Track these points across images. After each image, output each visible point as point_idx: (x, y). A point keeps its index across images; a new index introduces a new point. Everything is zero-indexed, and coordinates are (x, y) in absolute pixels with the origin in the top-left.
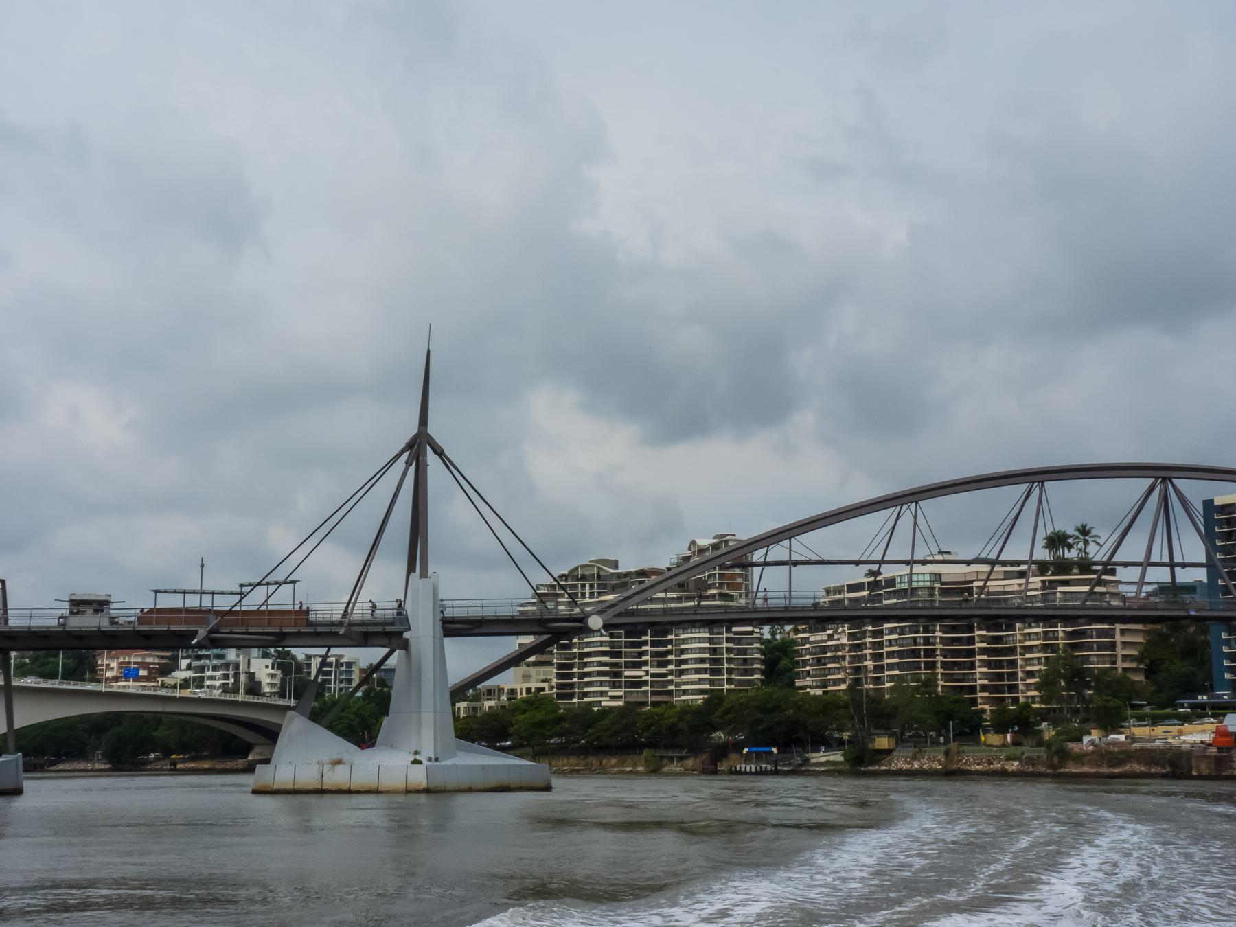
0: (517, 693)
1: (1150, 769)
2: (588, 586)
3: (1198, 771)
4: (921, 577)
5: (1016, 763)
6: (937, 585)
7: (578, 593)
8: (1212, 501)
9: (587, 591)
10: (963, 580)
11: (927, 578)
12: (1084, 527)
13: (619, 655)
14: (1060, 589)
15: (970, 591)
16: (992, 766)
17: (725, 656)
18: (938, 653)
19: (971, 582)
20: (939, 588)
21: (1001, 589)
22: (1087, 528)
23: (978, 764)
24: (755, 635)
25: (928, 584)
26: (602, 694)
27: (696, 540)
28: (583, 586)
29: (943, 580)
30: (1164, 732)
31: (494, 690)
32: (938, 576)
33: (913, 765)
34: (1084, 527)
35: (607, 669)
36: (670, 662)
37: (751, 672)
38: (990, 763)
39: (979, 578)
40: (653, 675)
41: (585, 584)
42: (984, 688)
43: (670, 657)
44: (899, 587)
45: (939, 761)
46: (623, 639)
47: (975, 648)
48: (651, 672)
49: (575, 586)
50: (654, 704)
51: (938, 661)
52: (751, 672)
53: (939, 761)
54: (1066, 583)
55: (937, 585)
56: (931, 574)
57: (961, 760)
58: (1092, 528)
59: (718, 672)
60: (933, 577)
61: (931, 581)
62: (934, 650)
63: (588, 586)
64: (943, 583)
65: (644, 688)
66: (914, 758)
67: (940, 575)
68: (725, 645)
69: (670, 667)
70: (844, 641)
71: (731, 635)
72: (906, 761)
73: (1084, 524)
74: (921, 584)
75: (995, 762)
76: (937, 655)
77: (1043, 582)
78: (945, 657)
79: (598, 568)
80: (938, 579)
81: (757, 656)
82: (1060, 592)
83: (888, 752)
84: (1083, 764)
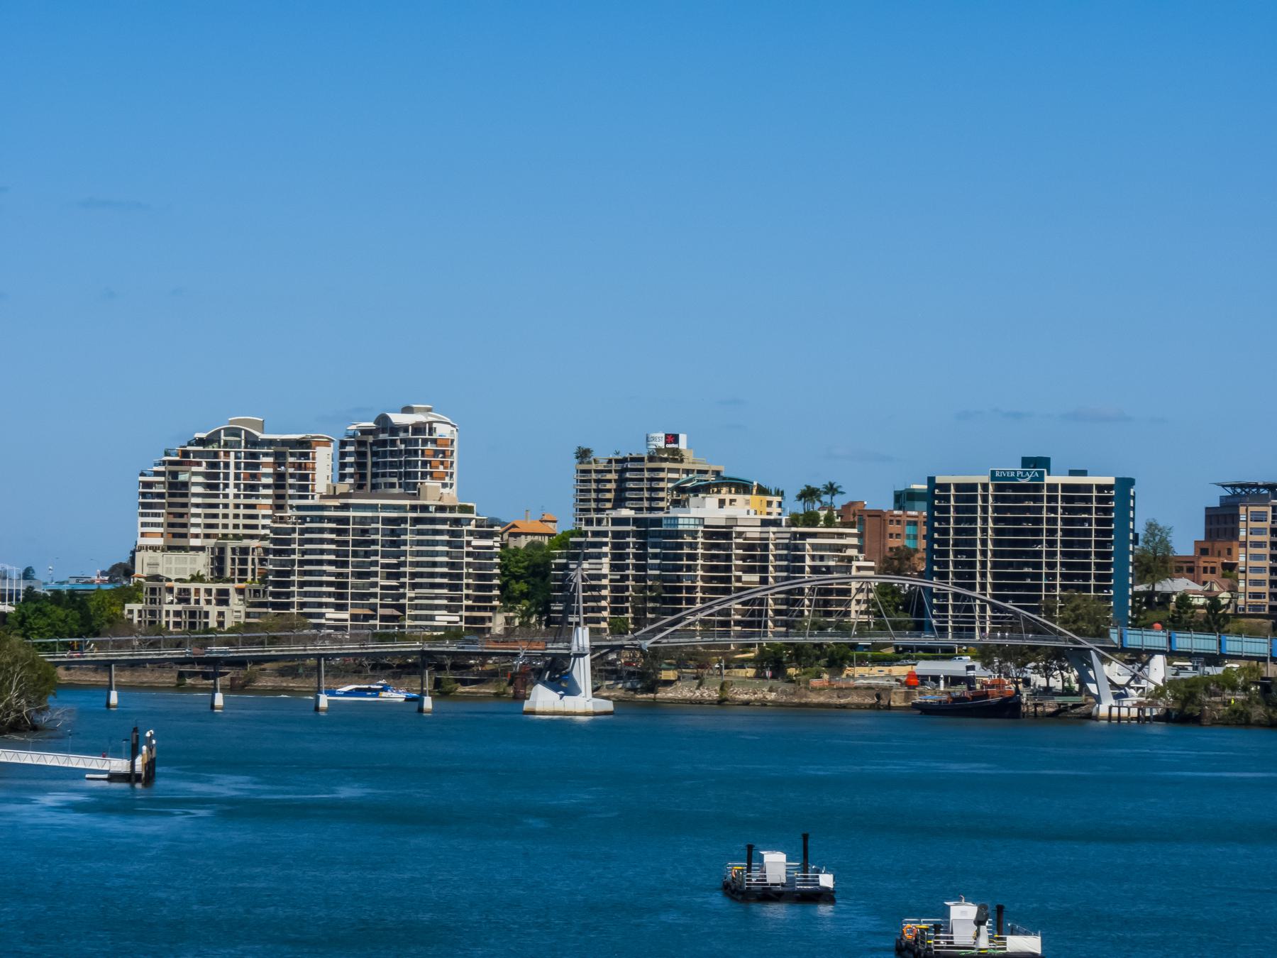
0: (190, 594)
1: (864, 700)
2: (232, 454)
3: (894, 702)
4: (686, 521)
5: (774, 694)
6: (701, 528)
7: (219, 462)
9: (232, 460)
10: (724, 524)
12: (832, 485)
13: (345, 564)
14: (809, 541)
15: (727, 536)
16: (756, 696)
17: (465, 571)
18: (699, 589)
19: (731, 527)
20: (702, 531)
21: (757, 535)
22: (835, 486)
23: (746, 694)
24: (496, 550)
25: (692, 528)
26: (327, 605)
27: (390, 415)
28: (227, 454)
29: (706, 524)
30: (879, 671)
31: (160, 589)
32: (702, 520)
33: (695, 693)
34: (832, 485)
35: (333, 579)
36: (404, 575)
37: (490, 588)
38: (755, 693)
39: (739, 524)
40: (383, 587)
41: (229, 452)
42: (738, 623)
43: (402, 569)
45: (715, 690)
46: (351, 548)
47: (731, 587)
48: (382, 583)
49: (216, 454)
50: (384, 618)
51: (697, 597)
52: (490, 588)
53: (715, 690)
54: (814, 535)
55: (701, 528)
56: (695, 518)
57: (733, 690)
58: (840, 486)
59: (457, 587)
62: (695, 587)
63: (232, 454)
64: (706, 527)
65: (372, 601)
66: (698, 688)
67: (703, 519)
68: (466, 560)
69: (402, 580)
70: (606, 570)
71: (471, 549)
72: (689, 689)
73: (832, 482)
74: (686, 528)
76: (697, 592)
77: (795, 533)
78: (704, 594)
79: (246, 431)
80: (702, 523)
81: (497, 571)
82: (809, 544)
83: (669, 683)
84: (821, 695)
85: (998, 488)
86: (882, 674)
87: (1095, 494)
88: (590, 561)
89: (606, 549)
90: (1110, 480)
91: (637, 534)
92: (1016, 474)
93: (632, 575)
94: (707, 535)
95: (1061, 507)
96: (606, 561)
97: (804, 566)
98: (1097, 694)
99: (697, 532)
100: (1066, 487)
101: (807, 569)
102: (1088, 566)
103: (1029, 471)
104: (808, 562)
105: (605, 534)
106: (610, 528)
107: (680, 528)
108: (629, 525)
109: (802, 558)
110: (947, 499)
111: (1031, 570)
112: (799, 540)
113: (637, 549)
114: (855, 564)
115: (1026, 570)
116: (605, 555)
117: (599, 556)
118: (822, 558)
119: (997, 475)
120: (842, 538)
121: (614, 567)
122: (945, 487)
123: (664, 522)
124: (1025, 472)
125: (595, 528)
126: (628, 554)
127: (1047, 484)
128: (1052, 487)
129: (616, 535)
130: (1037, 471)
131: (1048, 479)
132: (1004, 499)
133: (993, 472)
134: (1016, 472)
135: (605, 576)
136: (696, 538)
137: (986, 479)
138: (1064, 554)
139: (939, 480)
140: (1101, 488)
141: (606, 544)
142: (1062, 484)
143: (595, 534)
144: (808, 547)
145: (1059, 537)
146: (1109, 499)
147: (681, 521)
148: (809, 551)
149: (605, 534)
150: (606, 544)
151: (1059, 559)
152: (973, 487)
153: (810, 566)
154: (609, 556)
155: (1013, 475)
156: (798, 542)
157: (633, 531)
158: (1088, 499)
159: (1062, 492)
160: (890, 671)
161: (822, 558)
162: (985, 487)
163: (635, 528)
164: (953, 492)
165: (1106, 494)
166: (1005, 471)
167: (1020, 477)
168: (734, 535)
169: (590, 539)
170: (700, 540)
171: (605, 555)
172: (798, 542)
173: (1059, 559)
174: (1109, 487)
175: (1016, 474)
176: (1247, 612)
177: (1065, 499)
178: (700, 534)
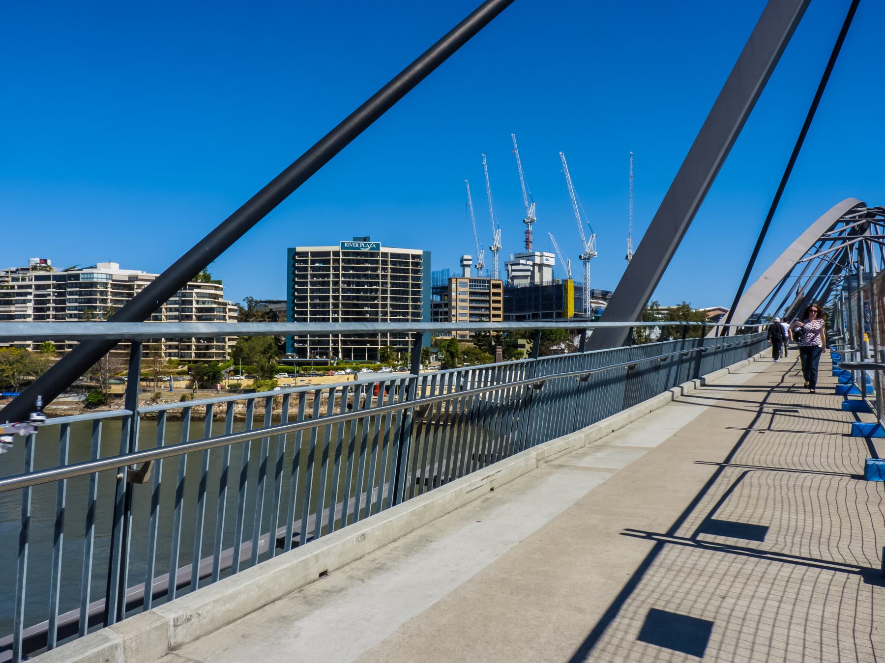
4: (100, 276)
6: (110, 282)
8: (295, 249)
11: (104, 276)
16: (221, 408)
20: (111, 284)
25: (104, 281)
32: (110, 276)
44: (81, 281)
54: (199, 287)
55: (110, 282)
56: (106, 274)
60: (108, 276)
61: (106, 279)
64: (113, 281)
67: (112, 275)
70: (30, 312)
74: (100, 280)
75: (223, 405)
85: (345, 254)
86: (303, 383)
87: (411, 260)
88: (16, 305)
89: (29, 297)
90: (419, 252)
91: (55, 287)
92: (359, 245)
93: (52, 314)
94: (114, 286)
95: (391, 268)
96: (31, 305)
97: (192, 308)
98: (858, 413)
99: (107, 284)
100: (393, 255)
101: (194, 310)
102: (407, 307)
103: (369, 244)
104: (195, 305)
105: (30, 287)
106: (34, 283)
107: (95, 280)
108: (50, 280)
109: (191, 302)
110: (306, 262)
111: (370, 309)
112: (189, 290)
113: (56, 296)
114: (229, 307)
115: (366, 309)
116: (30, 301)
117: (24, 302)
118: (204, 303)
119: (346, 245)
120: (217, 290)
121: (36, 309)
122: (305, 254)
123: (82, 276)
124: (366, 244)
125: (21, 283)
126: (49, 300)
127: (382, 253)
128: (385, 255)
129: (38, 287)
130: (375, 244)
131: (383, 250)
132: (349, 261)
133: (343, 244)
134: (359, 244)
135: (29, 316)
136: (107, 288)
137: (337, 248)
138: (392, 299)
139: (299, 249)
140: (414, 257)
141: (30, 294)
142: (391, 254)
143: (20, 287)
144: (194, 295)
145: (389, 288)
146: (417, 264)
147: (95, 275)
148: (195, 298)
149: (30, 287)
150: (30, 294)
151: (389, 302)
152: (327, 254)
153: (196, 308)
154: (33, 302)
155: (357, 245)
156: (187, 291)
157: (53, 284)
158: (407, 264)
159: (391, 258)
160: (310, 380)
161: (204, 303)
162: (336, 254)
163: (55, 282)
164: (310, 258)
165: (416, 261)
166: (351, 243)
167: (362, 247)
168: (135, 287)
169: (16, 290)
170: (110, 290)
171: (30, 301)
172: (187, 291)
173: (389, 302)
174: (418, 257)
175: (359, 245)
176: (458, 338)
177: (393, 263)
178: (109, 286)
